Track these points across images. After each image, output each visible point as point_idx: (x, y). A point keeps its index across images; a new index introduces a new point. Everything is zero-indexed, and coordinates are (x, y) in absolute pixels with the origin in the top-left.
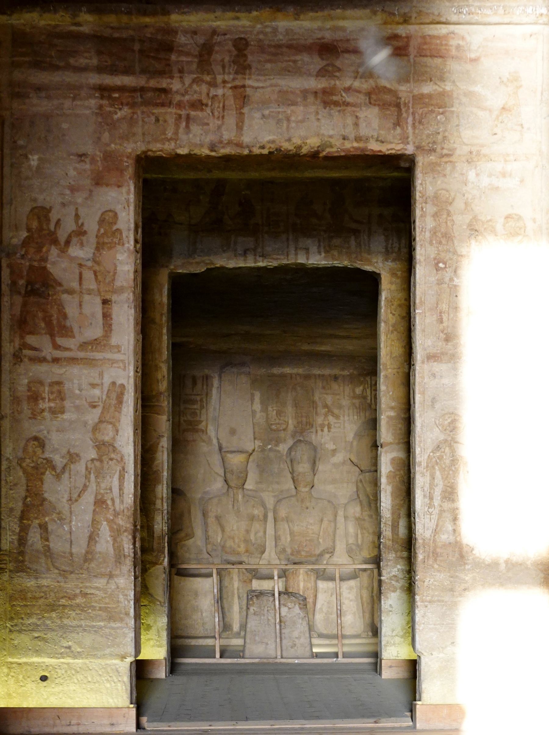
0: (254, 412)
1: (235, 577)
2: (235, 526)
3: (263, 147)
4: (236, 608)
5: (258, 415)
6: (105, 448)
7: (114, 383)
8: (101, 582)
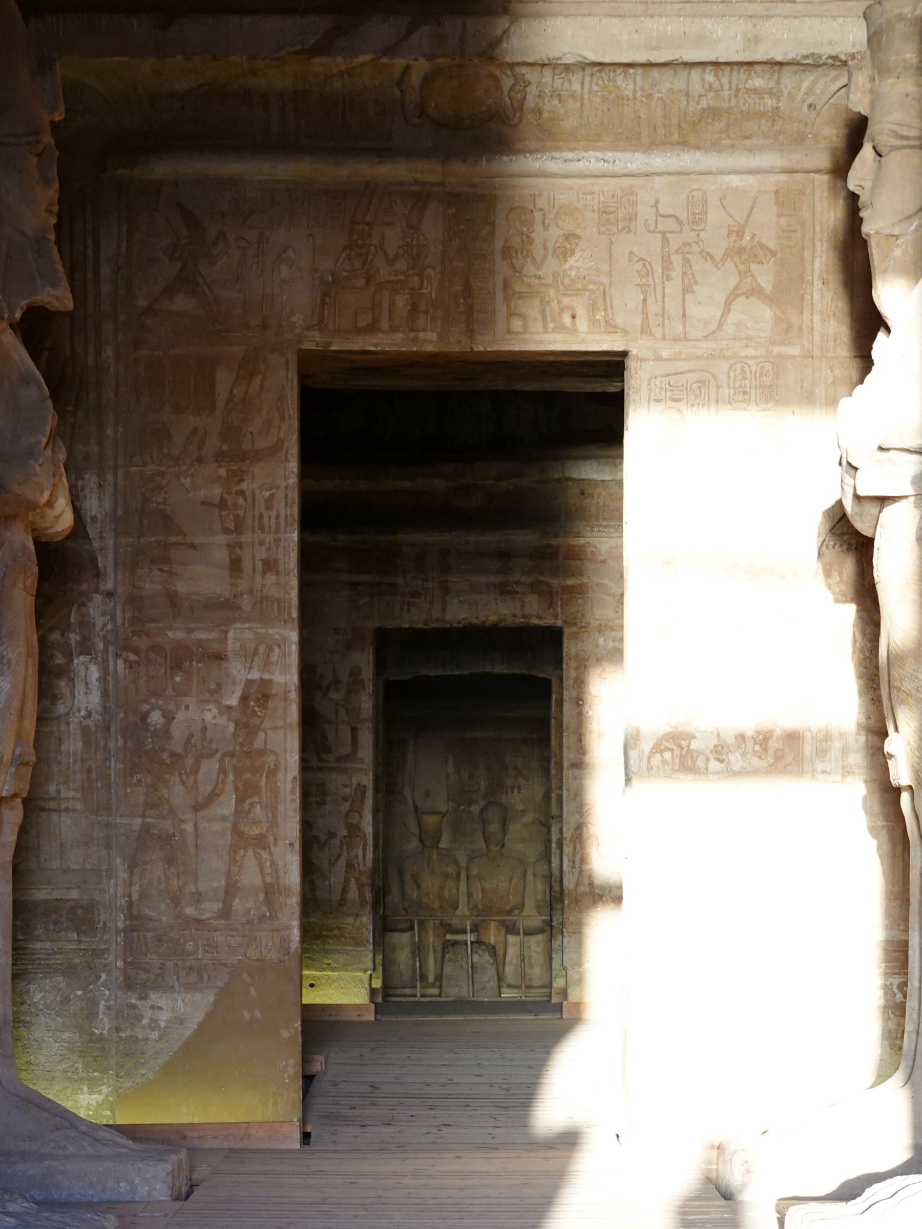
0: (448, 775)
1: (431, 932)
2: (430, 883)
3: (459, 623)
4: (431, 960)
5: (452, 777)
6: (354, 829)
7: (359, 785)
8: (350, 920)
